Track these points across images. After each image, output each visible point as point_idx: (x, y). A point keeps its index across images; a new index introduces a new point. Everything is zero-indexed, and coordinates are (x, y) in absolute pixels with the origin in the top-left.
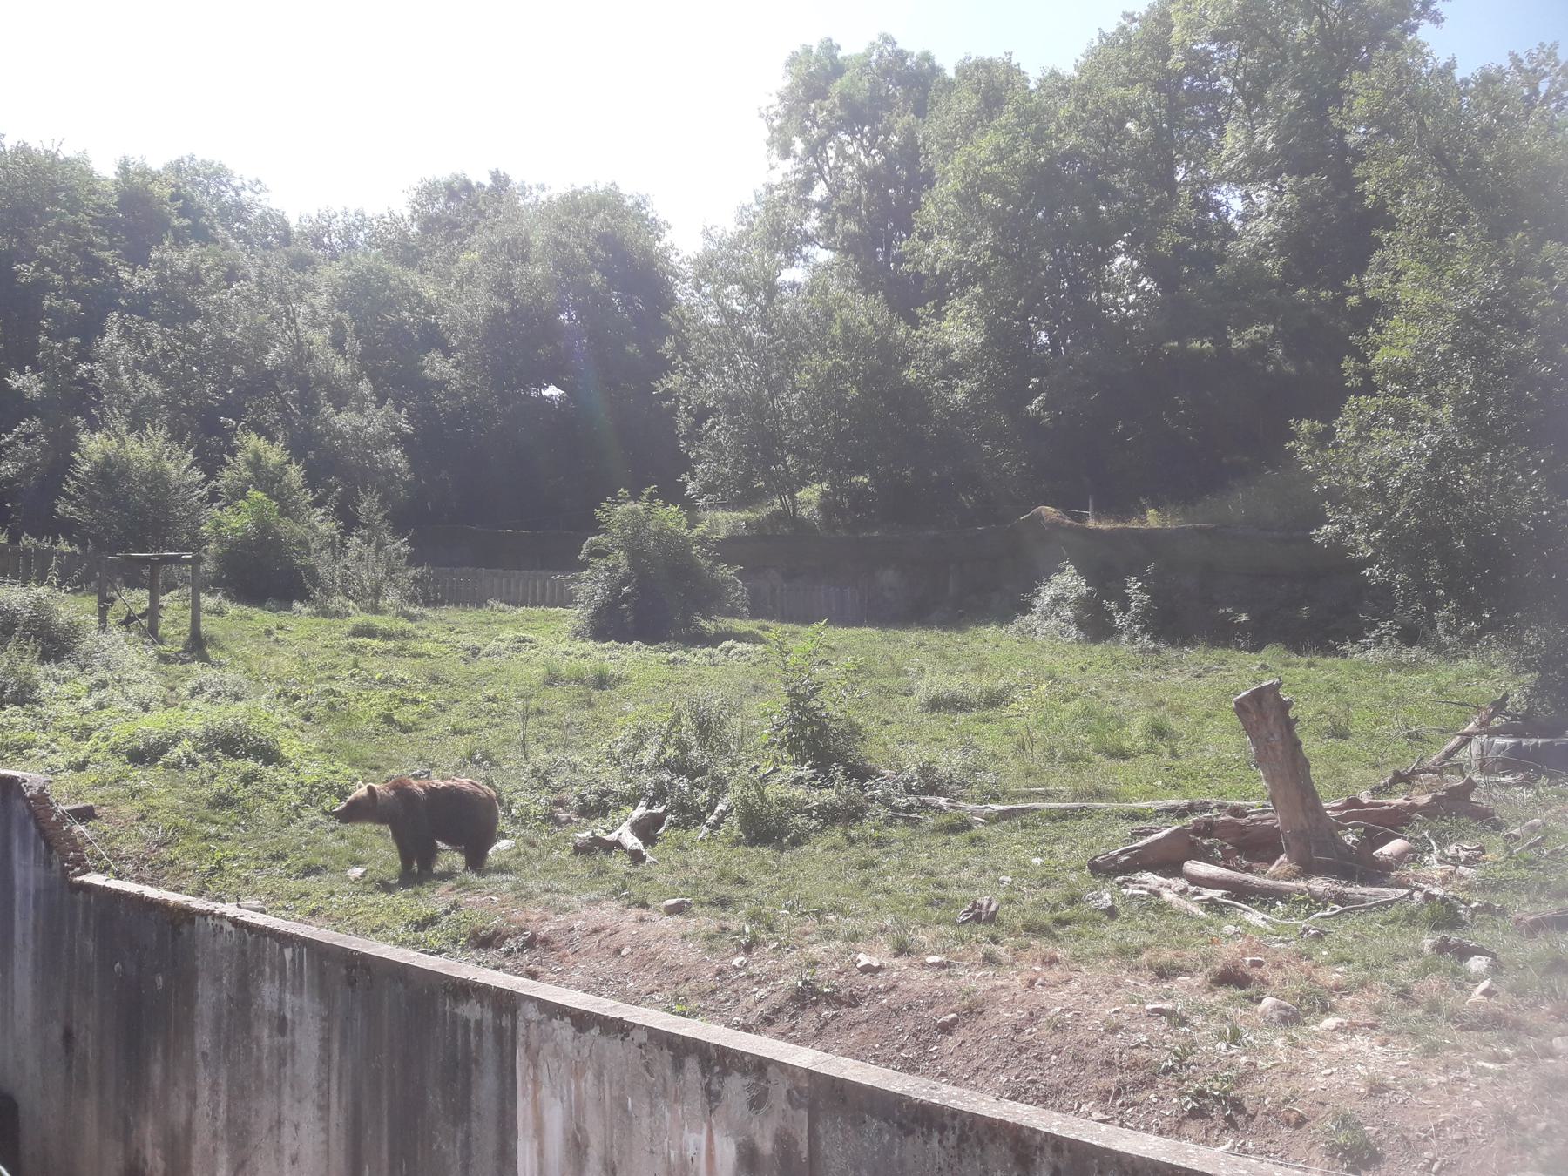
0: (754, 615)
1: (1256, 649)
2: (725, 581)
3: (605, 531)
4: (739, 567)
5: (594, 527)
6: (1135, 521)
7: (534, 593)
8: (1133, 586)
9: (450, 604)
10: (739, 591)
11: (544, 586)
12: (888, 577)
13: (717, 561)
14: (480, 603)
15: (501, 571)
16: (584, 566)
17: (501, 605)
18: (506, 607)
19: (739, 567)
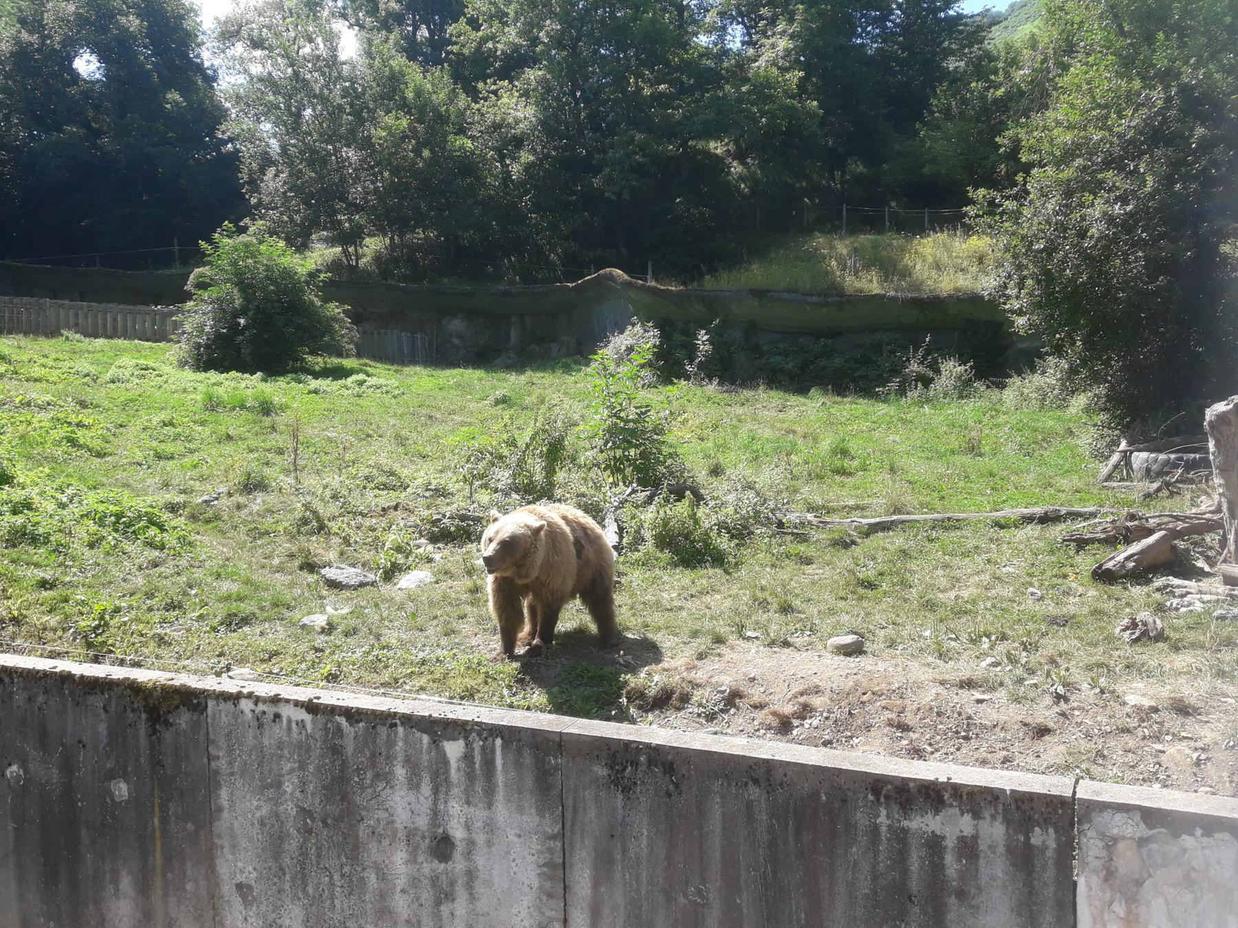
0: (359, 355)
1: (803, 390)
2: (334, 319)
3: (210, 263)
4: (346, 307)
5: (199, 258)
6: (695, 284)
7: (105, 325)
8: (703, 336)
9: (16, 333)
10: (346, 331)
11: (115, 320)
12: (456, 325)
13: (326, 300)
14: (53, 333)
15: (67, 302)
16: (188, 296)
17: (78, 336)
18: (82, 337)
19: (346, 307)
